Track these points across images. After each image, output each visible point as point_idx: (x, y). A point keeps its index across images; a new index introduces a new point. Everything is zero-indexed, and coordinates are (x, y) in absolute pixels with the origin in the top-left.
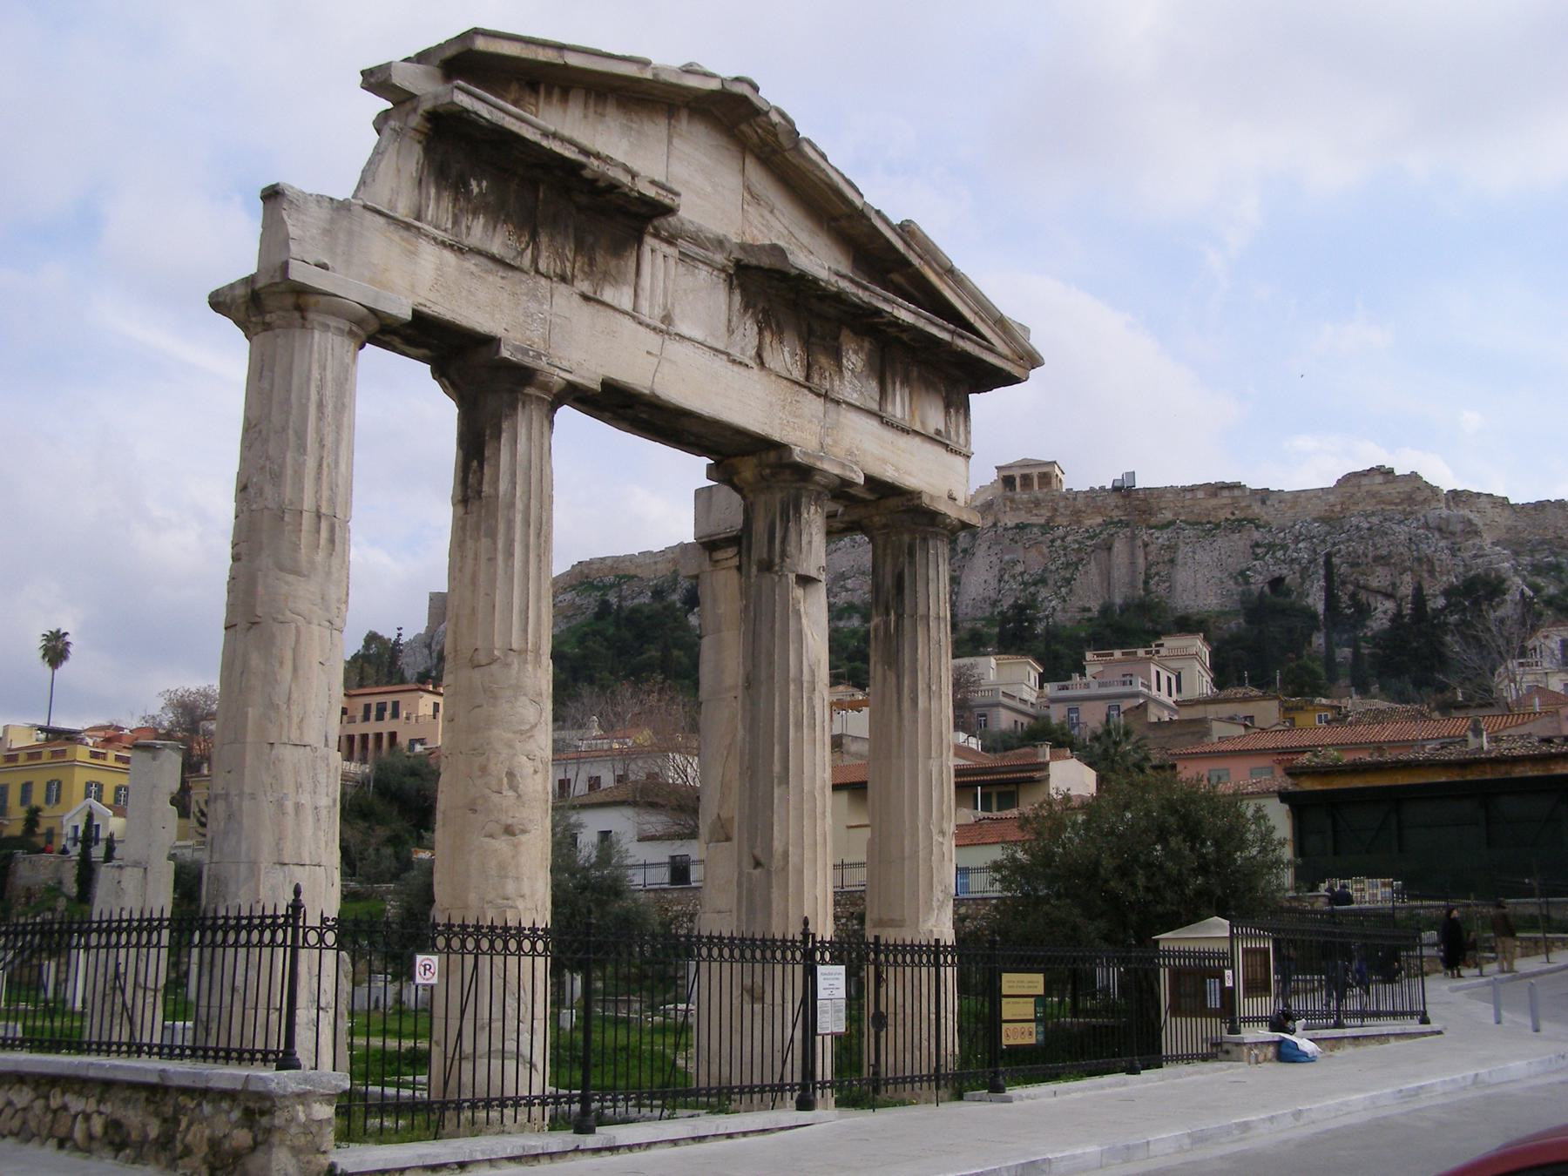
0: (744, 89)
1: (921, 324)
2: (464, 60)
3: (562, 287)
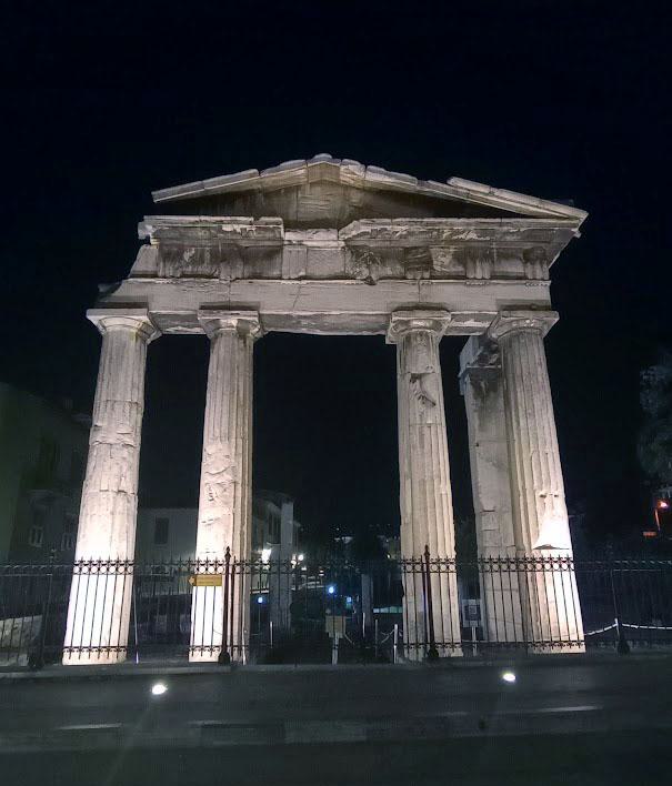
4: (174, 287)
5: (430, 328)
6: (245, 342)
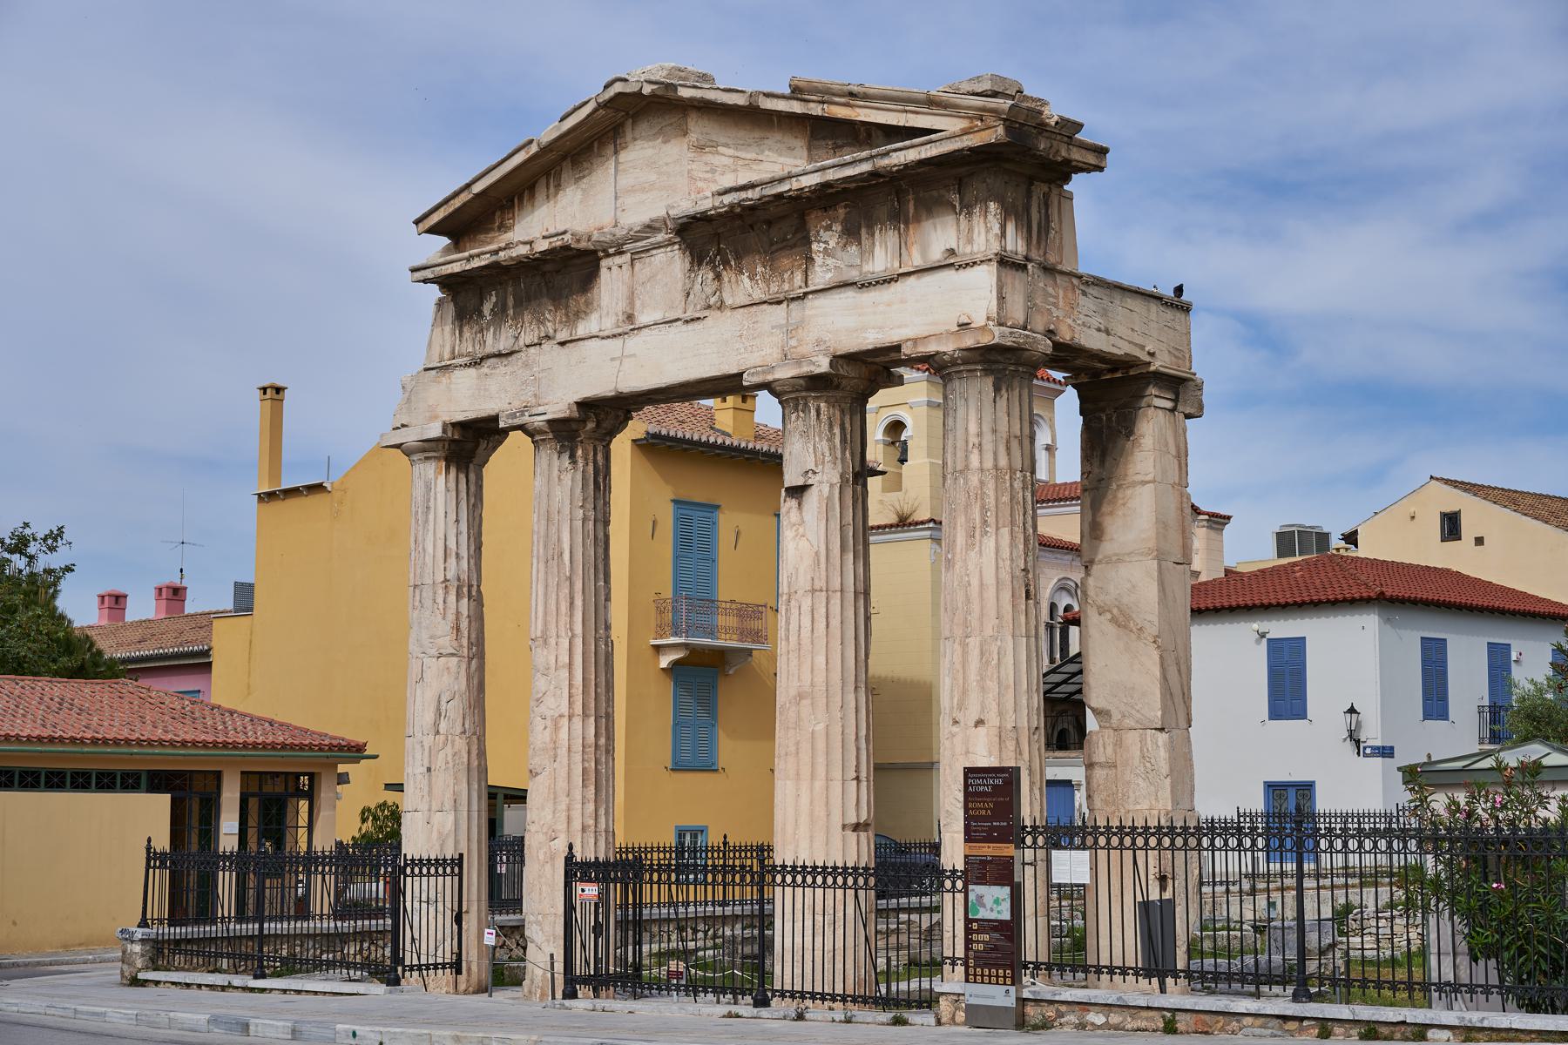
0: (618, 88)
1: (832, 175)
2: (463, 222)
3: (546, 346)
4: (472, 371)
5: (808, 389)
6: (572, 457)
